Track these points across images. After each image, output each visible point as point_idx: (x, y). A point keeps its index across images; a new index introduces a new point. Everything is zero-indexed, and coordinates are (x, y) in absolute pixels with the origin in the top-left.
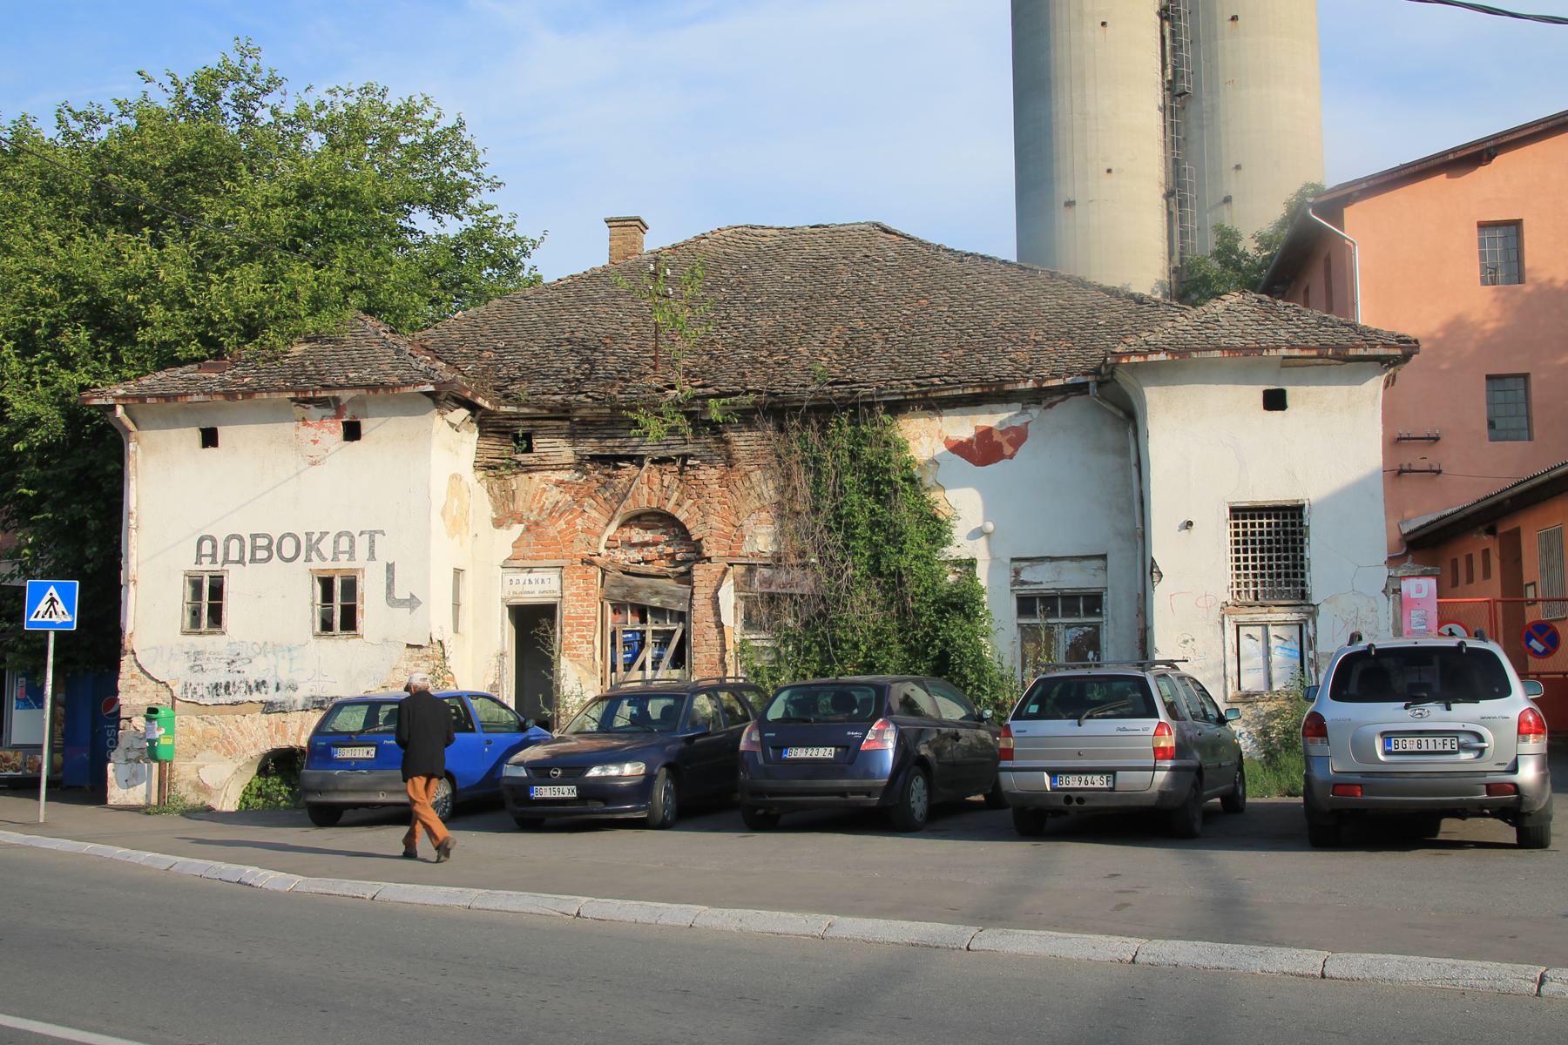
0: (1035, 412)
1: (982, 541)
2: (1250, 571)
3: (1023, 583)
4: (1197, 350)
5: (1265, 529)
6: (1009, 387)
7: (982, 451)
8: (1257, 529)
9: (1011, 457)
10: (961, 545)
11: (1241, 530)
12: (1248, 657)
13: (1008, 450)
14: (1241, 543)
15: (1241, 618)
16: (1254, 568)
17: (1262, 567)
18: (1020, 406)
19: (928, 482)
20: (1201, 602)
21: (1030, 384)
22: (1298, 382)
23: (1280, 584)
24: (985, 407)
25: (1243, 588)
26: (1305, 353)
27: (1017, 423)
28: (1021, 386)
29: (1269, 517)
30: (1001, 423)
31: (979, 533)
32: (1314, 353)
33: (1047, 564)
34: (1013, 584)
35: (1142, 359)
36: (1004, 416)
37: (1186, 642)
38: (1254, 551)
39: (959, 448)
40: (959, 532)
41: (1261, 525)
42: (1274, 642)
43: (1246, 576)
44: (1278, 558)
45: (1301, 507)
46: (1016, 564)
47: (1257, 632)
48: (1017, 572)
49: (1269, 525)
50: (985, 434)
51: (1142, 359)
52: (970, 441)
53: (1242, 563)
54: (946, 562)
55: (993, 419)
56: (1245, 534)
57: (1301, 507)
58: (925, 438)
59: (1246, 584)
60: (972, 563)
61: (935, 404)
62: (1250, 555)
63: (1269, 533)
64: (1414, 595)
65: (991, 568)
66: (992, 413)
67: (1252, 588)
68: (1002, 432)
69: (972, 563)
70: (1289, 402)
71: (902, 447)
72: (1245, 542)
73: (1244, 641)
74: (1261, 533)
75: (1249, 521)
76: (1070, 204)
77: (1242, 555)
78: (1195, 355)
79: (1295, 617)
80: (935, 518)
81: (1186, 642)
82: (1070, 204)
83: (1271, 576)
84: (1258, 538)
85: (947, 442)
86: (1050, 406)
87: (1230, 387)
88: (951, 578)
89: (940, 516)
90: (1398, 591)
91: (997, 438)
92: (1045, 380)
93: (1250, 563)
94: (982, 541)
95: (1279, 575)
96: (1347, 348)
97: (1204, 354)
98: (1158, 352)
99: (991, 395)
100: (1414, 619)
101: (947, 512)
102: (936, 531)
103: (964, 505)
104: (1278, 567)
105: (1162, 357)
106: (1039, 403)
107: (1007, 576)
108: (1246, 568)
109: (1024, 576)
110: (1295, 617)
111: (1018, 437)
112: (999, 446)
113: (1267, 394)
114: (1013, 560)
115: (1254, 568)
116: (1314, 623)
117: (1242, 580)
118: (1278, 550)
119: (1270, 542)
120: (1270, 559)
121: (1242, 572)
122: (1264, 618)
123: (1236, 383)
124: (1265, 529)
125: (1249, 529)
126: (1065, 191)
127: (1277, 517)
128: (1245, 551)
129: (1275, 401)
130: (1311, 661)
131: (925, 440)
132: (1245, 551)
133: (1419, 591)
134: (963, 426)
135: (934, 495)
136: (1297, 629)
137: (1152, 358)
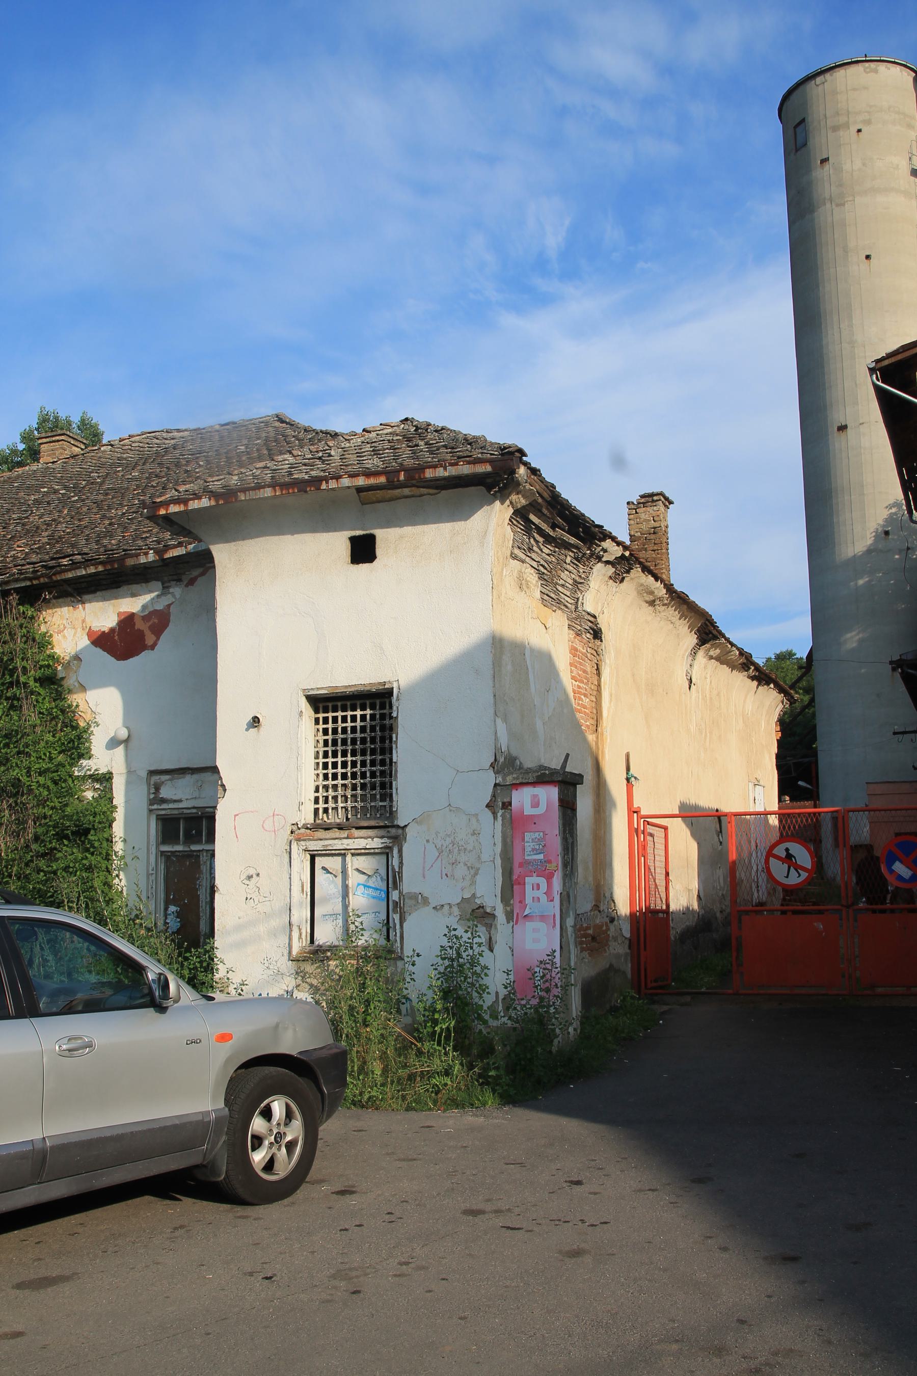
0: (177, 590)
1: (120, 750)
2: (340, 782)
3: (163, 801)
4: (244, 490)
5: (358, 723)
6: (130, 562)
7: (122, 642)
8: (349, 724)
9: (152, 647)
10: (103, 757)
11: (330, 726)
12: (326, 900)
13: (150, 639)
14: (334, 745)
15: (314, 846)
16: (344, 776)
17: (354, 775)
18: (159, 584)
19: (70, 682)
20: (268, 825)
21: (151, 556)
22: (388, 524)
23: (373, 798)
24: (125, 588)
25: (331, 804)
26: (372, 481)
27: (159, 607)
28: (143, 560)
29: (363, 708)
30: (144, 607)
31: (113, 743)
32: (382, 480)
33: (189, 779)
34: (152, 802)
35: (182, 508)
36: (146, 598)
37: (250, 877)
38: (344, 754)
39: (101, 641)
40: (98, 741)
41: (354, 719)
42: (354, 879)
43: (335, 787)
44: (373, 763)
45: (389, 693)
46: (155, 778)
47: (334, 863)
48: (157, 788)
49: (363, 718)
50: (127, 621)
51: (182, 508)
52: (112, 630)
53: (330, 771)
54: (84, 778)
55: (133, 604)
56: (335, 731)
57: (389, 693)
58: (70, 629)
59: (335, 798)
60: (106, 779)
61: (78, 590)
62: (339, 759)
63: (363, 729)
64: (529, 811)
65: (128, 783)
66: (133, 595)
67: (340, 805)
68: (144, 618)
69: (106, 779)
70: (378, 552)
71: (44, 643)
72: (335, 743)
73: (319, 875)
74: (354, 729)
75: (340, 714)
76: (842, 428)
77: (330, 760)
78: (242, 497)
79: (376, 843)
80: (75, 728)
81: (250, 877)
82: (842, 428)
83: (363, 786)
84: (350, 736)
85: (90, 634)
86: (192, 582)
87: (308, 537)
88: (89, 795)
89: (82, 724)
90: (507, 805)
91: (139, 625)
92: (167, 548)
93: (340, 770)
94: (120, 750)
95: (373, 787)
96: (422, 469)
97: (252, 495)
98: (199, 498)
99: (139, 576)
100: (529, 846)
101: (88, 717)
102: (76, 744)
103: (103, 707)
104: (373, 775)
105: (205, 502)
106: (179, 580)
107: (142, 794)
108: (335, 777)
109: (164, 793)
110: (376, 843)
111: (159, 621)
112: (141, 635)
113: (353, 540)
114: (152, 773)
115: (344, 776)
116: (400, 852)
117: (331, 793)
118: (373, 752)
119: (363, 741)
120: (363, 764)
121: (330, 782)
122: (338, 845)
123: (314, 530)
124: (358, 723)
125: (340, 725)
126: (838, 417)
127: (373, 707)
128: (335, 755)
129: (363, 551)
130: (395, 903)
131: (68, 633)
132: (335, 755)
133: (535, 804)
134: (103, 614)
135: (76, 699)
136: (385, 857)
137: (194, 505)
